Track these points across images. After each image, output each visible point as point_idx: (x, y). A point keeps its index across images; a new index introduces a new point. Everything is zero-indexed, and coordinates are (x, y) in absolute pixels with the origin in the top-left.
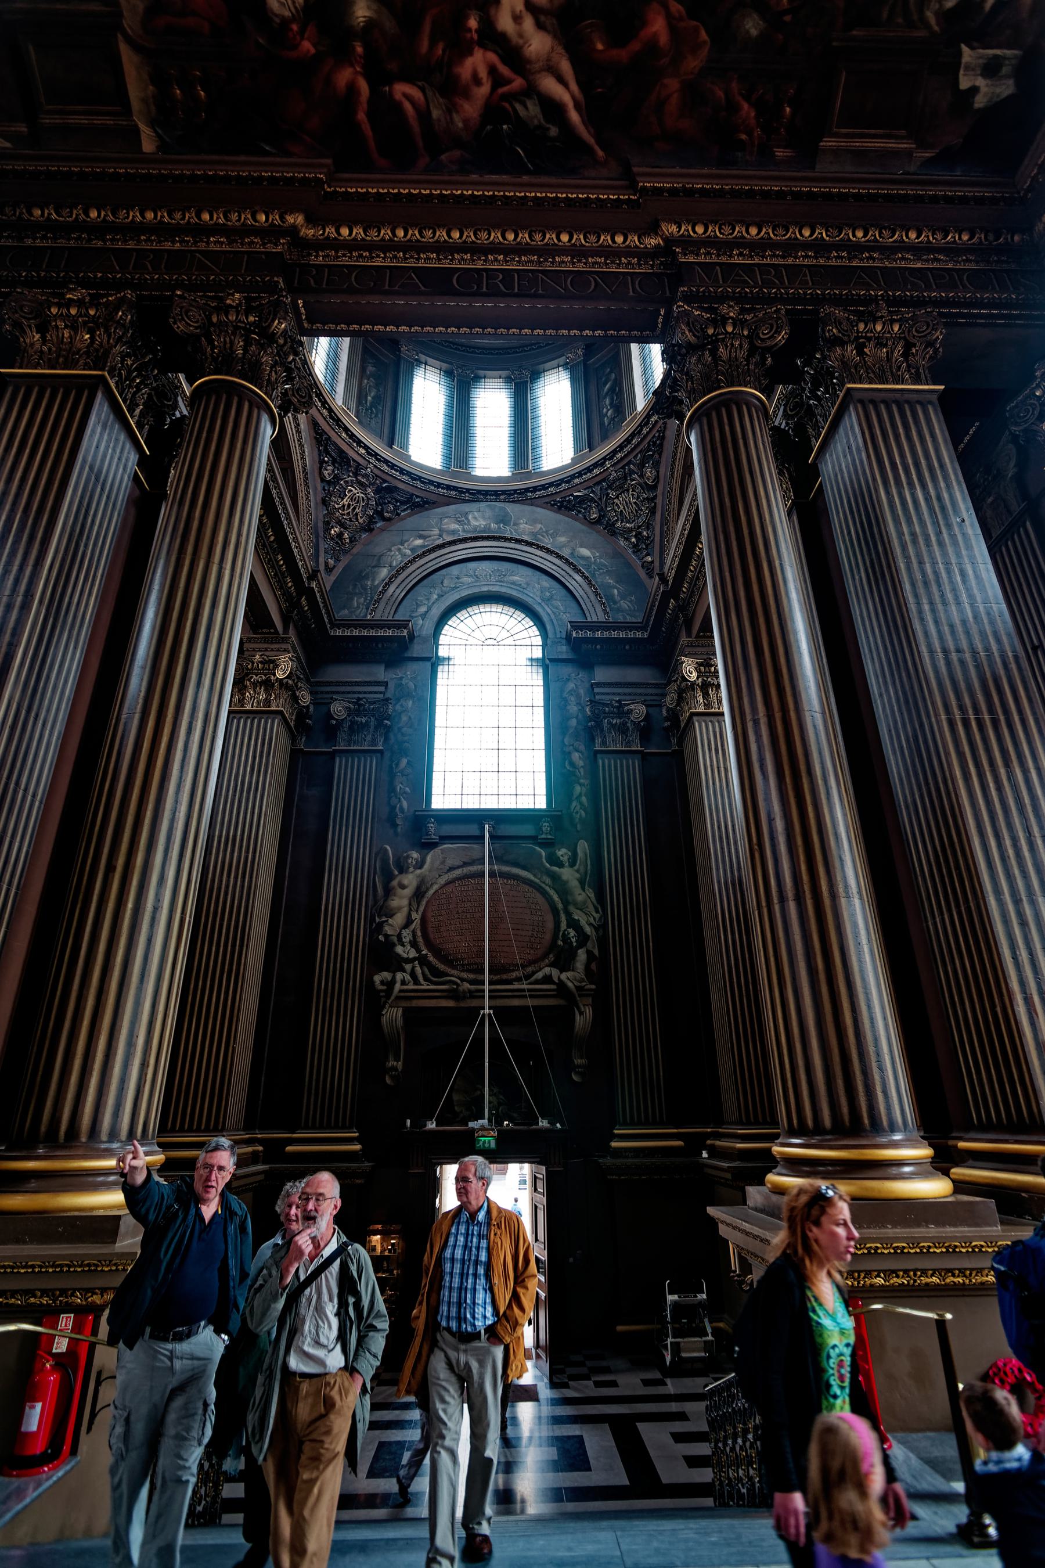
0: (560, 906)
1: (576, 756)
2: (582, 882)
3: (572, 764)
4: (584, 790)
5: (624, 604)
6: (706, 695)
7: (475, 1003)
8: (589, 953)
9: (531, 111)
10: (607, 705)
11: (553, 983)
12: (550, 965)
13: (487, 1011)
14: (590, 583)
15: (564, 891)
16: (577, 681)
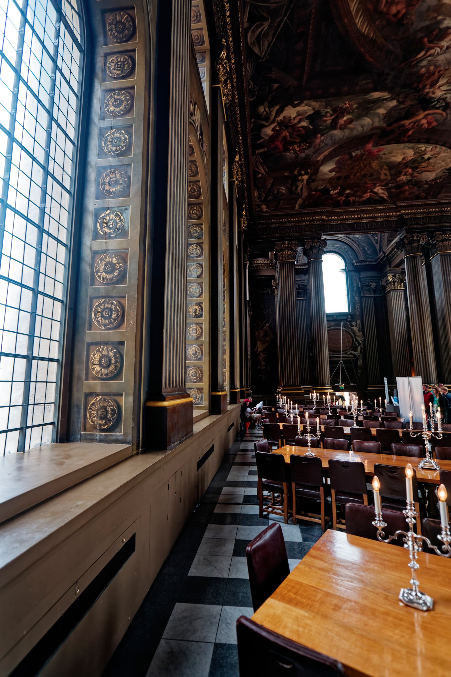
0: (354, 336)
1: (356, 298)
2: (359, 330)
3: (355, 300)
4: (359, 307)
5: (369, 252)
6: (394, 284)
7: (339, 359)
8: (361, 348)
9: (377, 198)
10: (365, 283)
11: (353, 354)
12: (352, 350)
13: (341, 362)
14: (359, 246)
15: (354, 333)
16: (356, 276)
